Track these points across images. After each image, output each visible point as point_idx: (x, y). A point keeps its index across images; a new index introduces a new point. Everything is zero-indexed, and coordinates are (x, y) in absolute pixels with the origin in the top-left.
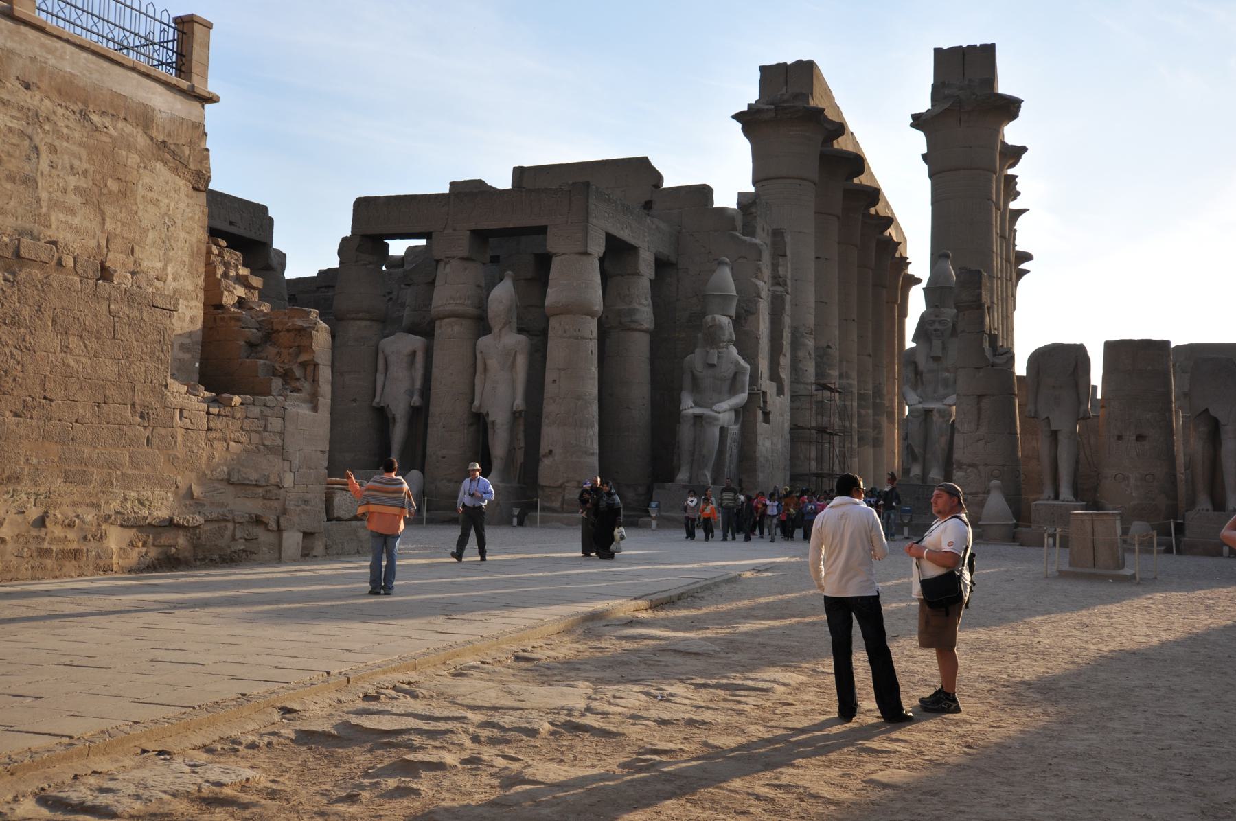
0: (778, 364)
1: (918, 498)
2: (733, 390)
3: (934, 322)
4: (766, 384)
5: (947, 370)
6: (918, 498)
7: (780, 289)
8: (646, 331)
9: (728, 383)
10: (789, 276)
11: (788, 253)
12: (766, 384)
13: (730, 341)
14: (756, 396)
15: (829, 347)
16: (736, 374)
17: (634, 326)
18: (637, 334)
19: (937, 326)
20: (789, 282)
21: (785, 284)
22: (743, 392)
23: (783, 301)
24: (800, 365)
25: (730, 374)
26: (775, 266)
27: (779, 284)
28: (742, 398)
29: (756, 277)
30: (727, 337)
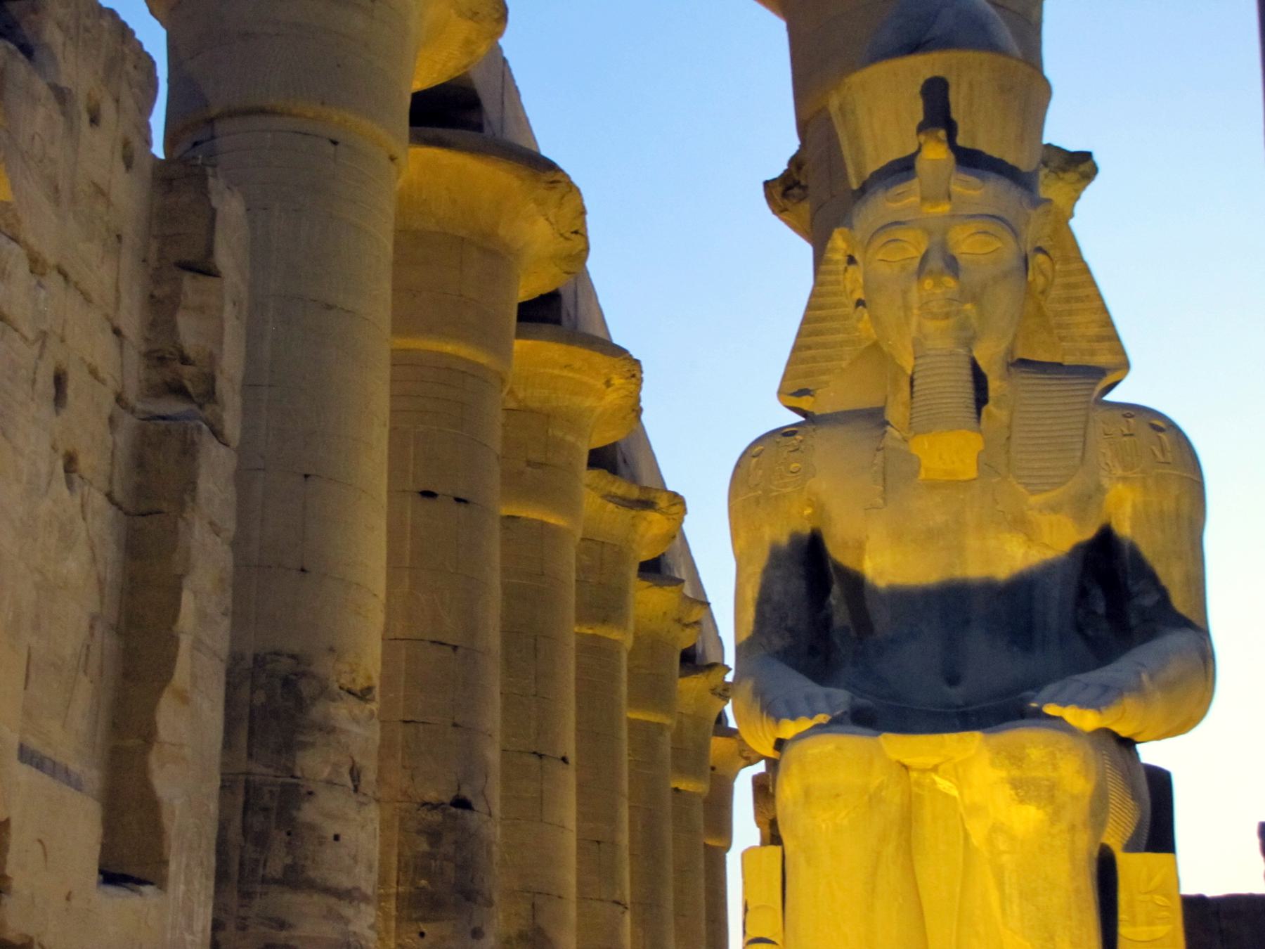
0: (149, 736)
10: (232, 364)
11: (223, 259)
21: (210, 395)
23: (189, 451)
24: (308, 813)
26: (161, 310)
27: (179, 391)
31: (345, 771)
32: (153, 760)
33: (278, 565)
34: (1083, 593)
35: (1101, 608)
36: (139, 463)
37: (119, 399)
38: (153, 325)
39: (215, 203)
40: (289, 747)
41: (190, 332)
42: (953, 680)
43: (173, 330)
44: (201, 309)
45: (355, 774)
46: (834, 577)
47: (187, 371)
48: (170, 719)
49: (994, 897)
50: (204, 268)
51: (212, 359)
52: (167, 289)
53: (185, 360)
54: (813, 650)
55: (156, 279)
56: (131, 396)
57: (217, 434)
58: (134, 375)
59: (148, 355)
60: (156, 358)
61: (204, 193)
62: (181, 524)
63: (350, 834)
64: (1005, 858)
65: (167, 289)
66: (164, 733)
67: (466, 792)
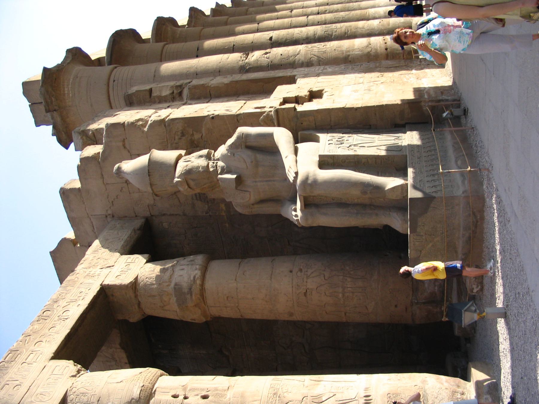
2: (270, 149)
4: (271, 103)
7: (186, 92)
8: (205, 270)
11: (148, 87)
12: (271, 103)
13: (208, 157)
14: (278, 118)
16: (249, 147)
17: (196, 289)
18: (209, 284)
20: (178, 83)
22: (271, 135)
23: (195, 87)
25: (247, 155)
27: (180, 94)
28: (282, 137)
29: (144, 126)
30: (202, 162)
31: (266, 56)
38: (166, 101)
39: (134, 91)
41: (166, 93)
43: (166, 96)
44: (161, 91)
45: (266, 53)
47: (175, 92)
50: (151, 91)
51: (172, 87)
52: (156, 99)
53: (173, 93)
57: (189, 83)
59: (173, 101)
61: (133, 94)
62: (212, 86)
63: (281, 52)
65: (156, 99)
67: (268, 38)
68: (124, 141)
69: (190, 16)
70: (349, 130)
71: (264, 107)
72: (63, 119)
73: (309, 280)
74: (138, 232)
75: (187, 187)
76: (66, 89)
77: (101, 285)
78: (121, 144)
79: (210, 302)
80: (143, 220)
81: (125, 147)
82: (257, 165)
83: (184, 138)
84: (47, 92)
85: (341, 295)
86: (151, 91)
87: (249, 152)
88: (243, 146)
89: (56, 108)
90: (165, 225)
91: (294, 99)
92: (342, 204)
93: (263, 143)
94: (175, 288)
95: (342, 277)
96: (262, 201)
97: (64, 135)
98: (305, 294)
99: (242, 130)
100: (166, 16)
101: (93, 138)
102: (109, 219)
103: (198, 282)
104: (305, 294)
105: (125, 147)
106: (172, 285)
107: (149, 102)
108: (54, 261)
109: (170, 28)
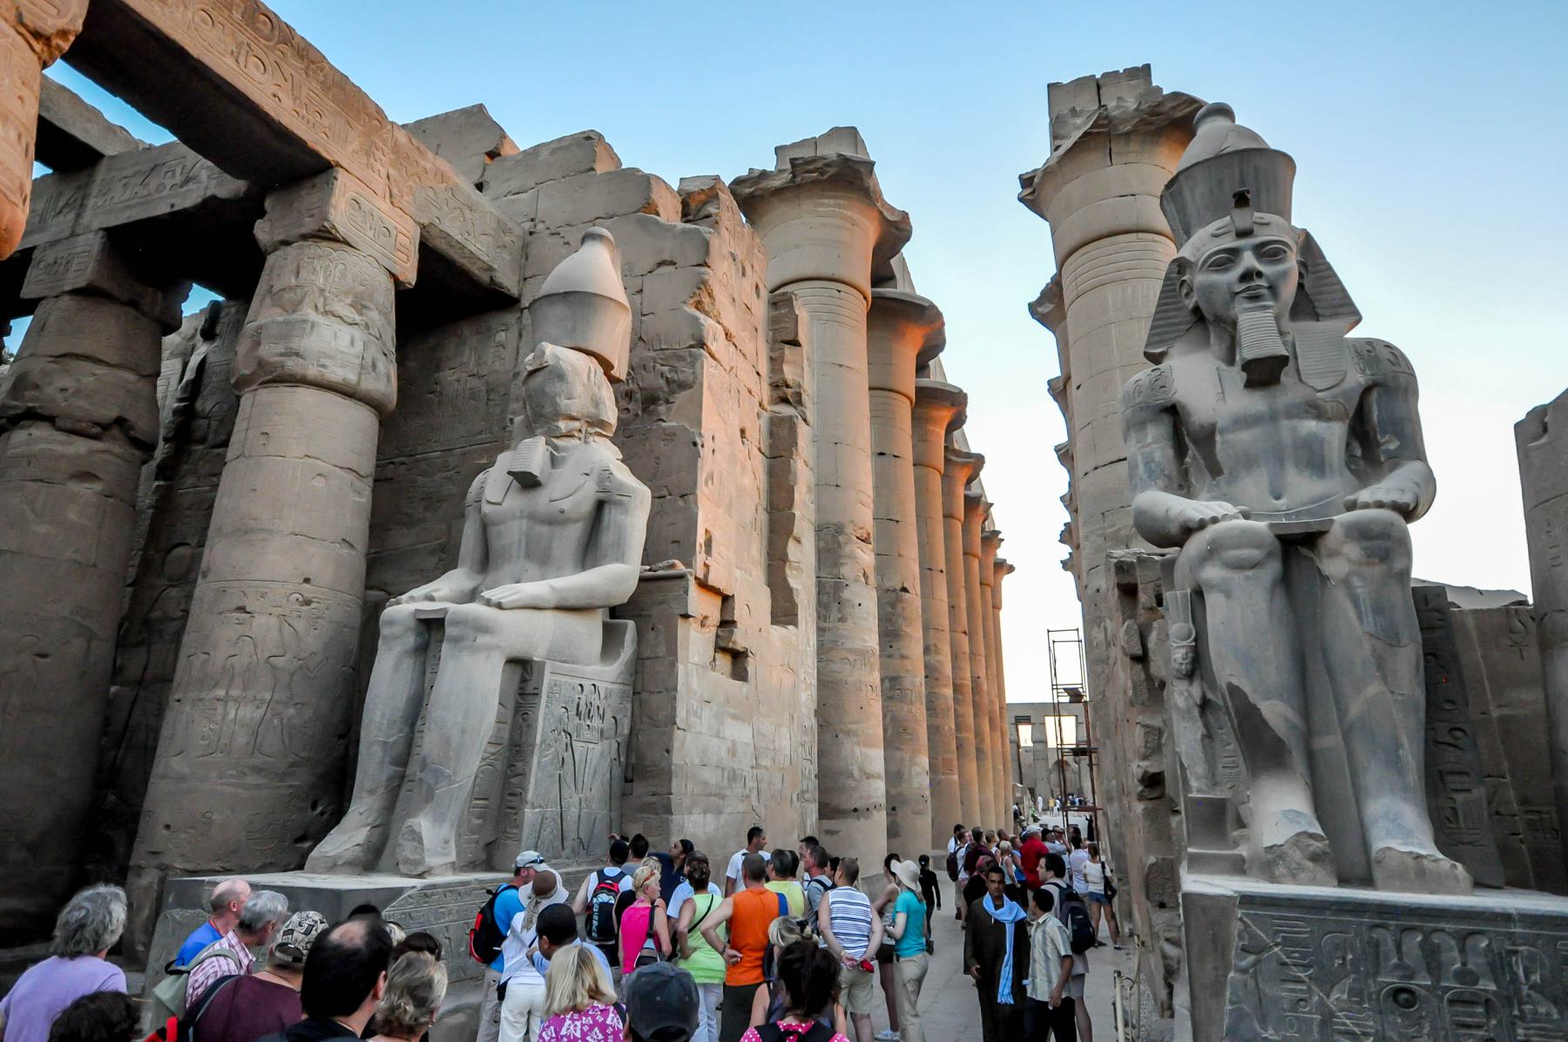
0: (784, 559)
1: (1403, 998)
3: (1234, 253)
5: (1316, 411)
6: (1403, 998)
7: (786, 410)
9: (574, 534)
11: (802, 338)
15: (904, 590)
16: (600, 506)
17: (292, 365)
18: (305, 395)
19: (1249, 260)
21: (800, 402)
22: (620, 558)
24: (846, 594)
26: (776, 362)
29: (698, 305)
32: (788, 571)
33: (829, 485)
34: (1348, 445)
35: (1358, 452)
36: (771, 434)
37: (761, 405)
40: (837, 565)
41: (789, 373)
42: (1278, 498)
43: (782, 372)
44: (794, 363)
46: (1190, 445)
47: (789, 391)
48: (792, 550)
49: (1352, 613)
50: (795, 343)
51: (800, 386)
54: (1181, 487)
55: (772, 350)
56: (765, 403)
58: (765, 392)
60: (775, 386)
61: (792, 307)
64: (1359, 591)
66: (791, 557)
68: (672, 263)
69: (969, 455)
70: (626, 731)
71: (708, 551)
72: (778, 192)
73: (273, 621)
74: (485, 278)
75: (530, 368)
76: (832, 201)
77: (338, 165)
78: (666, 257)
79: (266, 395)
80: (514, 291)
81: (660, 264)
82: (556, 520)
83: (662, 382)
84: (828, 165)
85: (221, 693)
86: (795, 343)
87: (587, 506)
88: (602, 496)
89: (798, 179)
90: (501, 336)
91: (728, 618)
92: (416, 710)
93: (607, 538)
94: (304, 321)
95: (268, 696)
96: (485, 526)
97: (748, 190)
98: (242, 609)
99: (641, 496)
100: (969, 410)
101: (702, 214)
102: (528, 226)
103: (312, 372)
104: (242, 609)
105: (660, 264)
106: (313, 316)
107: (775, 341)
108: (464, 112)
109: (946, 415)
